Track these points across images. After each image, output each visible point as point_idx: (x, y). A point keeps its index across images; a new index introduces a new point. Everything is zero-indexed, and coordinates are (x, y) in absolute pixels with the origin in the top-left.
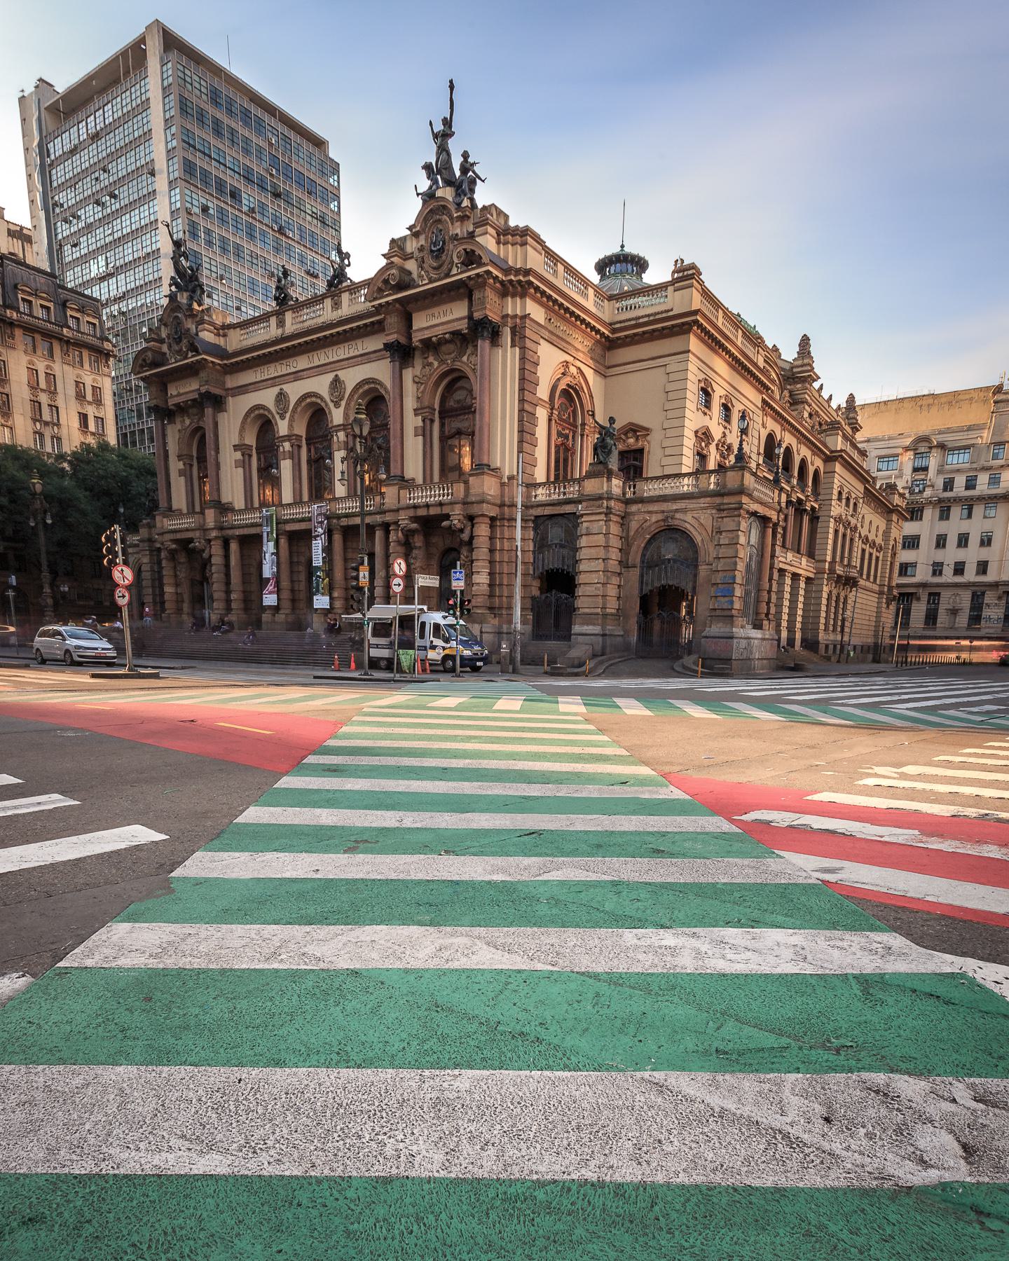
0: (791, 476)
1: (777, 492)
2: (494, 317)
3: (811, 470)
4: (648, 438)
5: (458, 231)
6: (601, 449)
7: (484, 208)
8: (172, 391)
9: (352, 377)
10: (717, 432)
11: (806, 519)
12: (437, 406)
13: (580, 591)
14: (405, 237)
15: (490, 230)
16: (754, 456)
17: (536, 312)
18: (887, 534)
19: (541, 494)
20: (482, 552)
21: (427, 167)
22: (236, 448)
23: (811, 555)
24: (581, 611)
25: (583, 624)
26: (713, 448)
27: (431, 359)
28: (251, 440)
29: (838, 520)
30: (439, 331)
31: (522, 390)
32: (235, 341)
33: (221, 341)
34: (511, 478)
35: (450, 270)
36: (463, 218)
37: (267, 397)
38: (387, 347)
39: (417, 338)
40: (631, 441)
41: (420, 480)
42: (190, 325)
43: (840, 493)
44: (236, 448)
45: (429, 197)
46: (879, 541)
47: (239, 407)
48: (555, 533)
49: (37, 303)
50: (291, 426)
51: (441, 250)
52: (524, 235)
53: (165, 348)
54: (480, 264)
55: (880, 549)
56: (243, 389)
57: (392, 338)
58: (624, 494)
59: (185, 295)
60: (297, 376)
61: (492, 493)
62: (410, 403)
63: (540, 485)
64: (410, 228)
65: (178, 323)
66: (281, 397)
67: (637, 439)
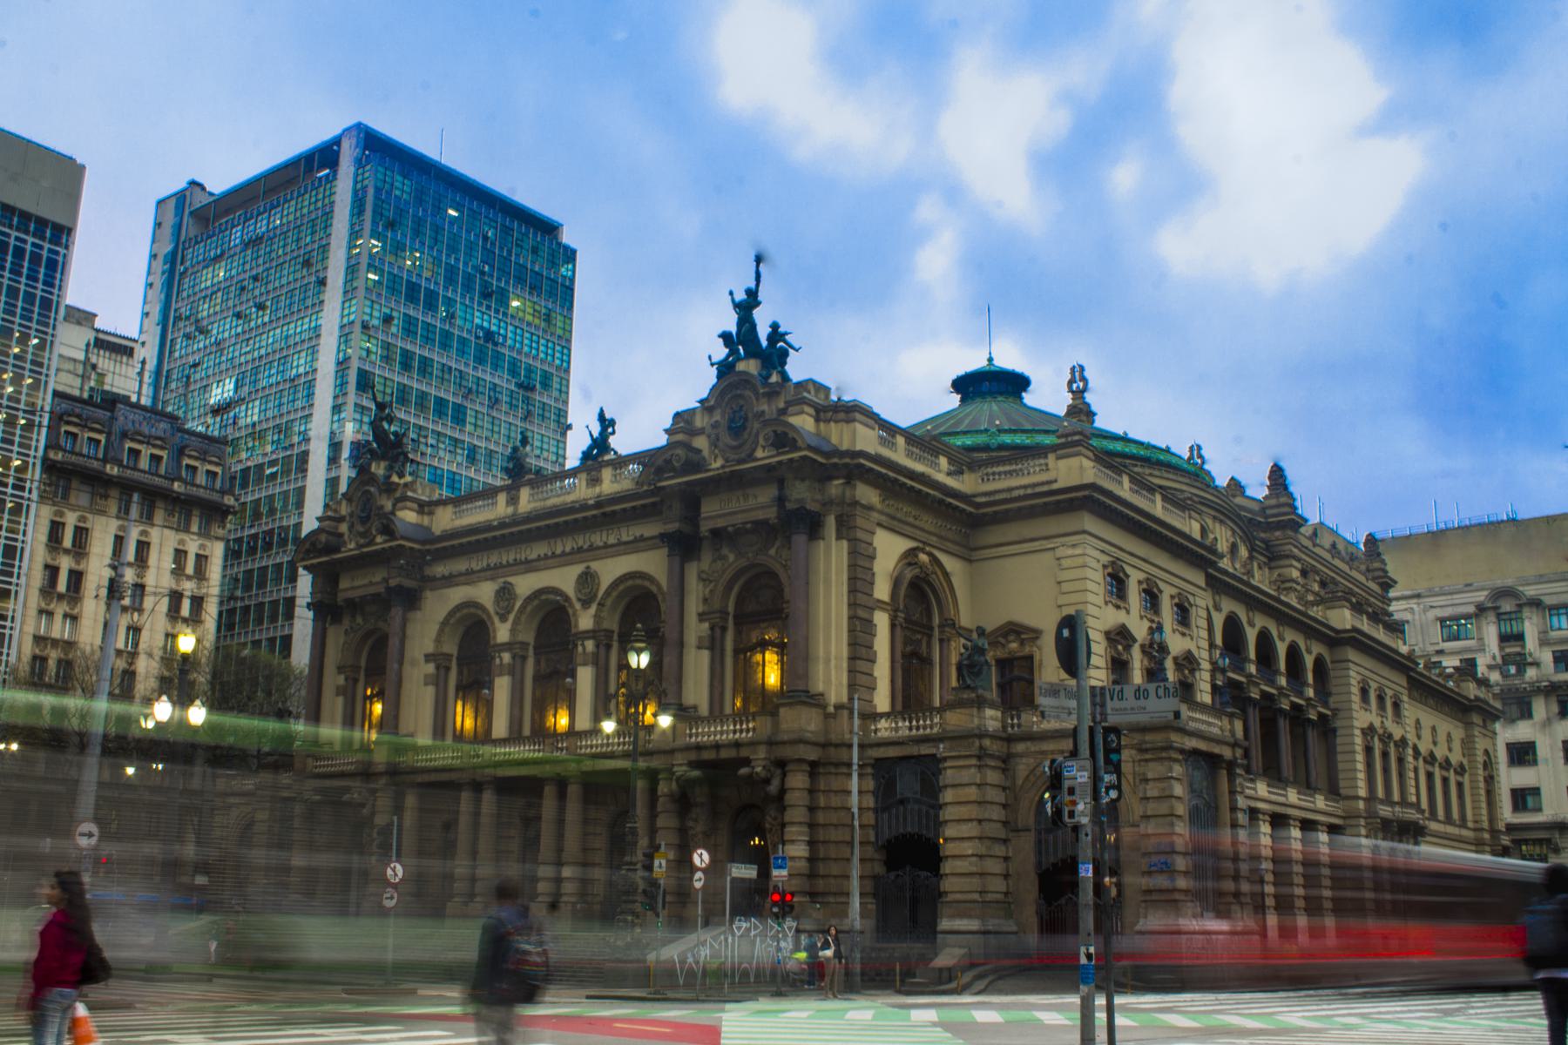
0: (1277, 672)
1: (1226, 721)
2: (812, 507)
3: (1309, 661)
4: (1039, 642)
5: (765, 407)
6: (970, 668)
7: (799, 385)
8: (344, 584)
9: (610, 570)
10: (1140, 630)
11: (1312, 736)
12: (731, 609)
13: (947, 867)
14: (694, 410)
15: (807, 409)
16: (1203, 656)
17: (867, 494)
18: (1468, 744)
19: (884, 728)
20: (796, 814)
21: (726, 337)
22: (428, 658)
23: (1333, 791)
24: (950, 897)
25: (952, 917)
26: (1136, 653)
27: (725, 551)
28: (451, 648)
29: (1369, 731)
30: (739, 519)
31: (852, 591)
32: (444, 520)
33: (426, 520)
34: (838, 707)
35: (754, 450)
36: (773, 393)
37: (485, 593)
38: (663, 537)
39: (705, 527)
40: (1014, 645)
41: (704, 710)
42: (388, 505)
43: (1364, 692)
44: (428, 658)
45: (725, 369)
46: (1456, 758)
47: (438, 606)
48: (907, 785)
49: (146, 451)
50: (513, 631)
51: (744, 428)
52: (852, 412)
53: (344, 528)
54: (796, 448)
55: (1461, 770)
56: (450, 581)
57: (673, 527)
58: (1004, 727)
59: (383, 464)
60: (529, 566)
61: (812, 727)
62: (693, 606)
63: (882, 715)
64: (701, 402)
65: (368, 499)
66: (505, 593)
67: (1022, 643)
